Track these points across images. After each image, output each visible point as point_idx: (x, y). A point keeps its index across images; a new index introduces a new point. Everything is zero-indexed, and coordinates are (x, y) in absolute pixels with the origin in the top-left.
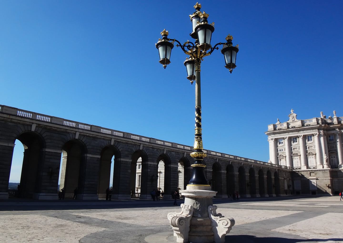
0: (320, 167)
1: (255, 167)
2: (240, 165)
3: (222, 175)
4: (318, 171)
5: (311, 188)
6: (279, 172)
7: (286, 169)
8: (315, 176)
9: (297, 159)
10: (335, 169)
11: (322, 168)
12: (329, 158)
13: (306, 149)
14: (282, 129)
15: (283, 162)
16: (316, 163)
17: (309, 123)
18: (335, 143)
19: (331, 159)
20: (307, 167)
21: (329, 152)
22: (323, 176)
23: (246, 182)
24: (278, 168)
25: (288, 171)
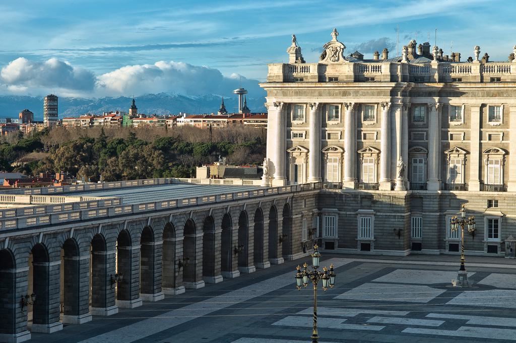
0: (385, 188)
1: (250, 206)
2: (225, 212)
3: (197, 242)
5: (360, 238)
6: (293, 202)
8: (372, 208)
10: (418, 191)
11: (389, 188)
12: (410, 163)
13: (359, 137)
14: (305, 80)
18: (426, 128)
21: (409, 147)
23: (233, 245)
24: (292, 195)
25: (310, 195)
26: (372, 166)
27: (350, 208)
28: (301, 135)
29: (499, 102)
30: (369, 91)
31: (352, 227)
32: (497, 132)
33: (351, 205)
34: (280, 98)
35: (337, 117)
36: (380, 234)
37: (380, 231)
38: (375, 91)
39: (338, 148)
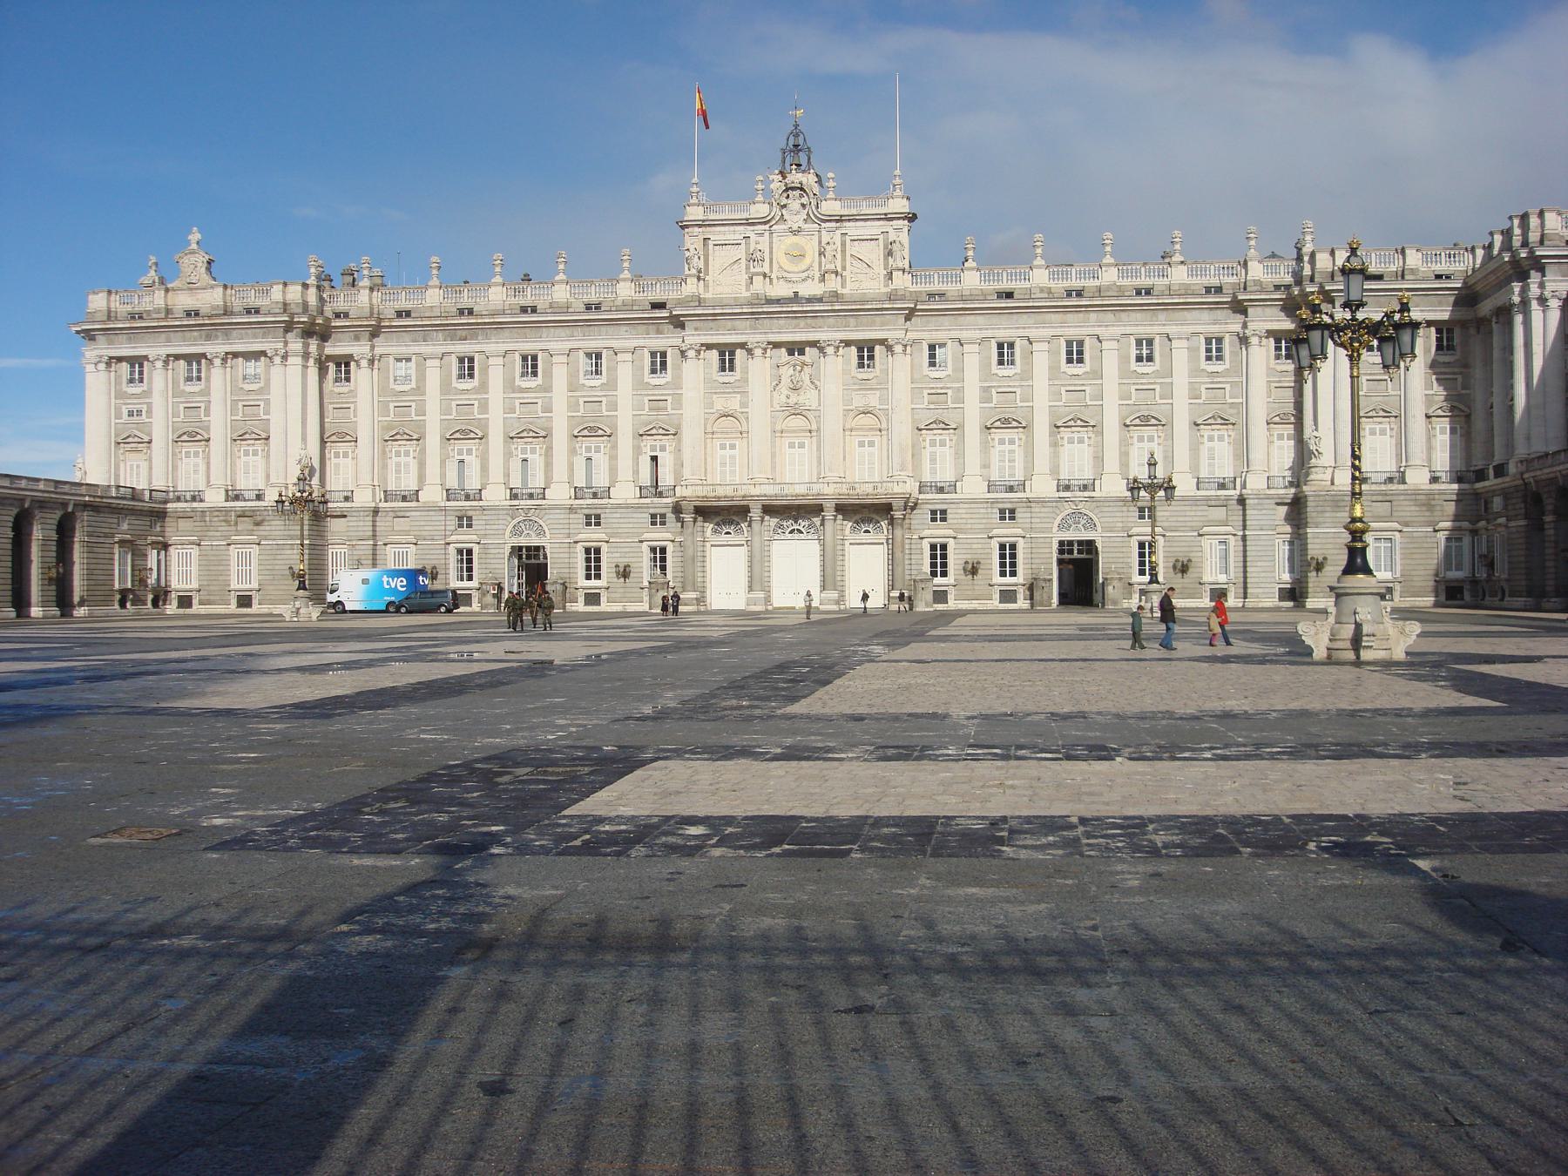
4: (266, 513)
5: (234, 585)
7: (133, 499)
8: (255, 533)
9: (196, 454)
14: (144, 316)
15: (138, 466)
16: (268, 476)
17: (259, 303)
19: (337, 461)
20: (227, 491)
22: (286, 533)
26: (259, 461)
27: (219, 534)
28: (139, 412)
29: (471, 350)
30: (249, 331)
31: (221, 568)
32: (469, 399)
33: (220, 529)
34: (102, 349)
35: (199, 379)
36: (267, 577)
37: (267, 573)
38: (258, 330)
39: (200, 431)
